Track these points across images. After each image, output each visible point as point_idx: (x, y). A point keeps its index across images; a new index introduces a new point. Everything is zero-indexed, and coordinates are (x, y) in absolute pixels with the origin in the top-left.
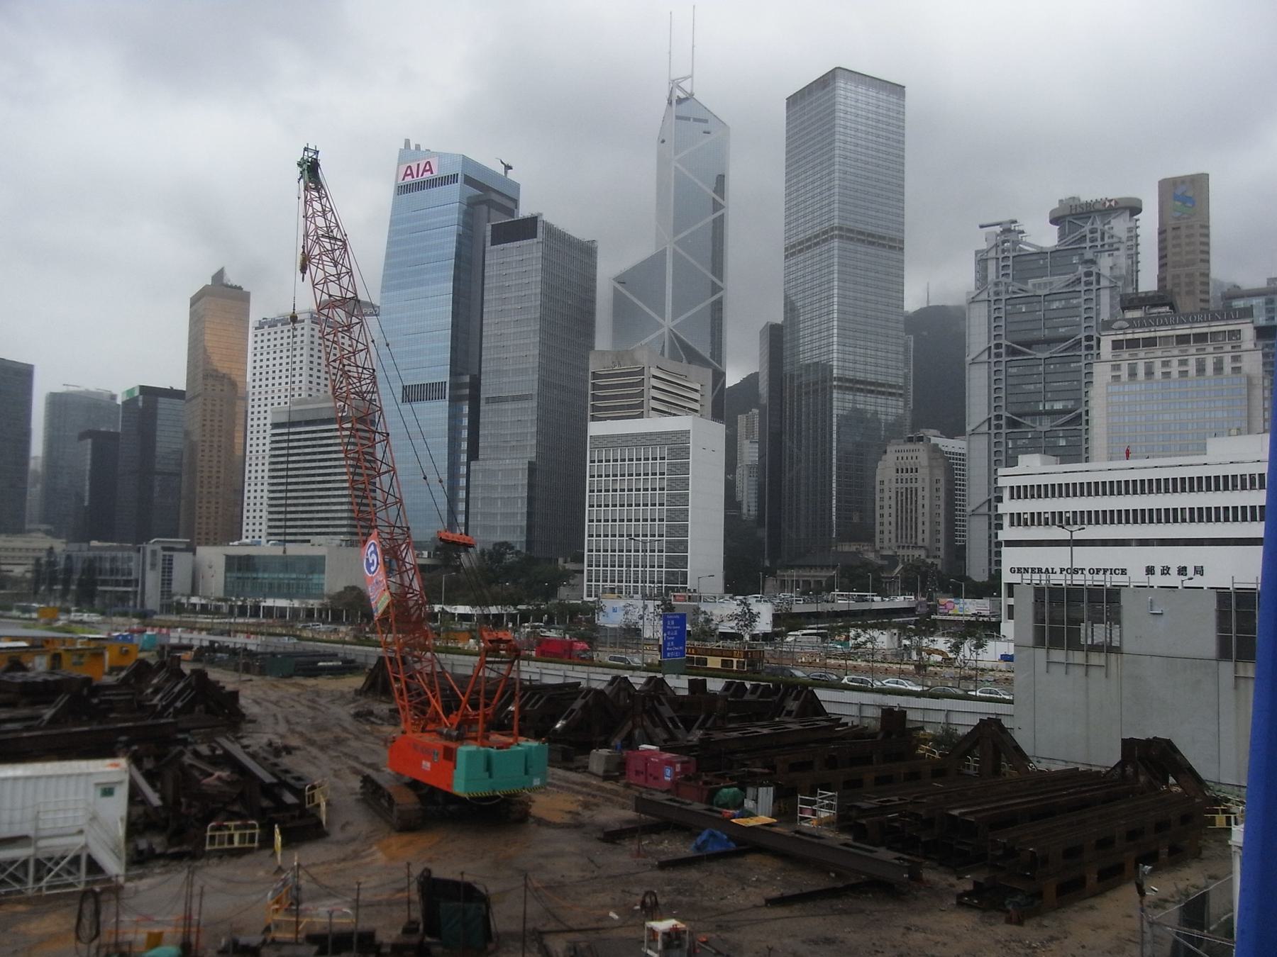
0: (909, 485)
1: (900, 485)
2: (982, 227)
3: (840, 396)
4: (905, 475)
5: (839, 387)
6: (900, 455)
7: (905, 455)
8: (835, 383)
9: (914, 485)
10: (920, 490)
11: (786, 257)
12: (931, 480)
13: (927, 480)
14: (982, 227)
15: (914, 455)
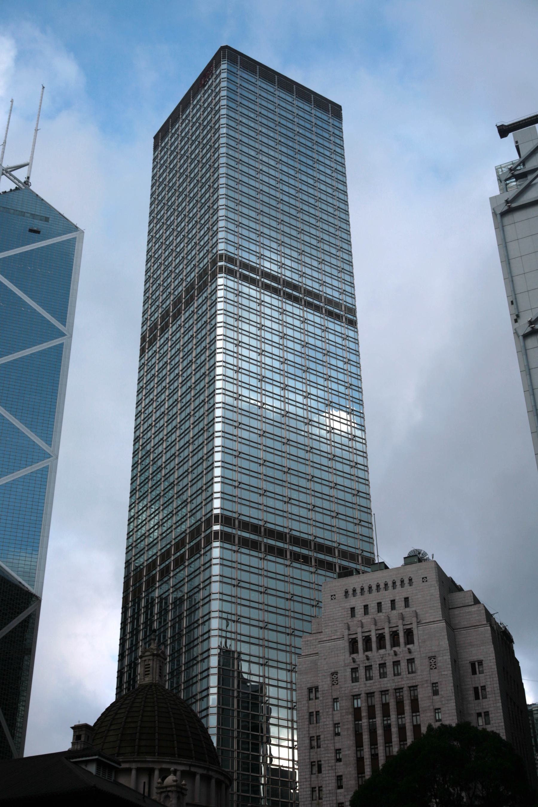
0: (389, 683)
1: (362, 687)
2: (504, 131)
3: (228, 555)
4: (376, 656)
5: (226, 538)
6: (358, 602)
7: (372, 600)
8: (216, 528)
9: (405, 681)
10: (424, 693)
11: (143, 351)
12: (455, 662)
13: (445, 659)
14: (504, 131)
15: (399, 594)
